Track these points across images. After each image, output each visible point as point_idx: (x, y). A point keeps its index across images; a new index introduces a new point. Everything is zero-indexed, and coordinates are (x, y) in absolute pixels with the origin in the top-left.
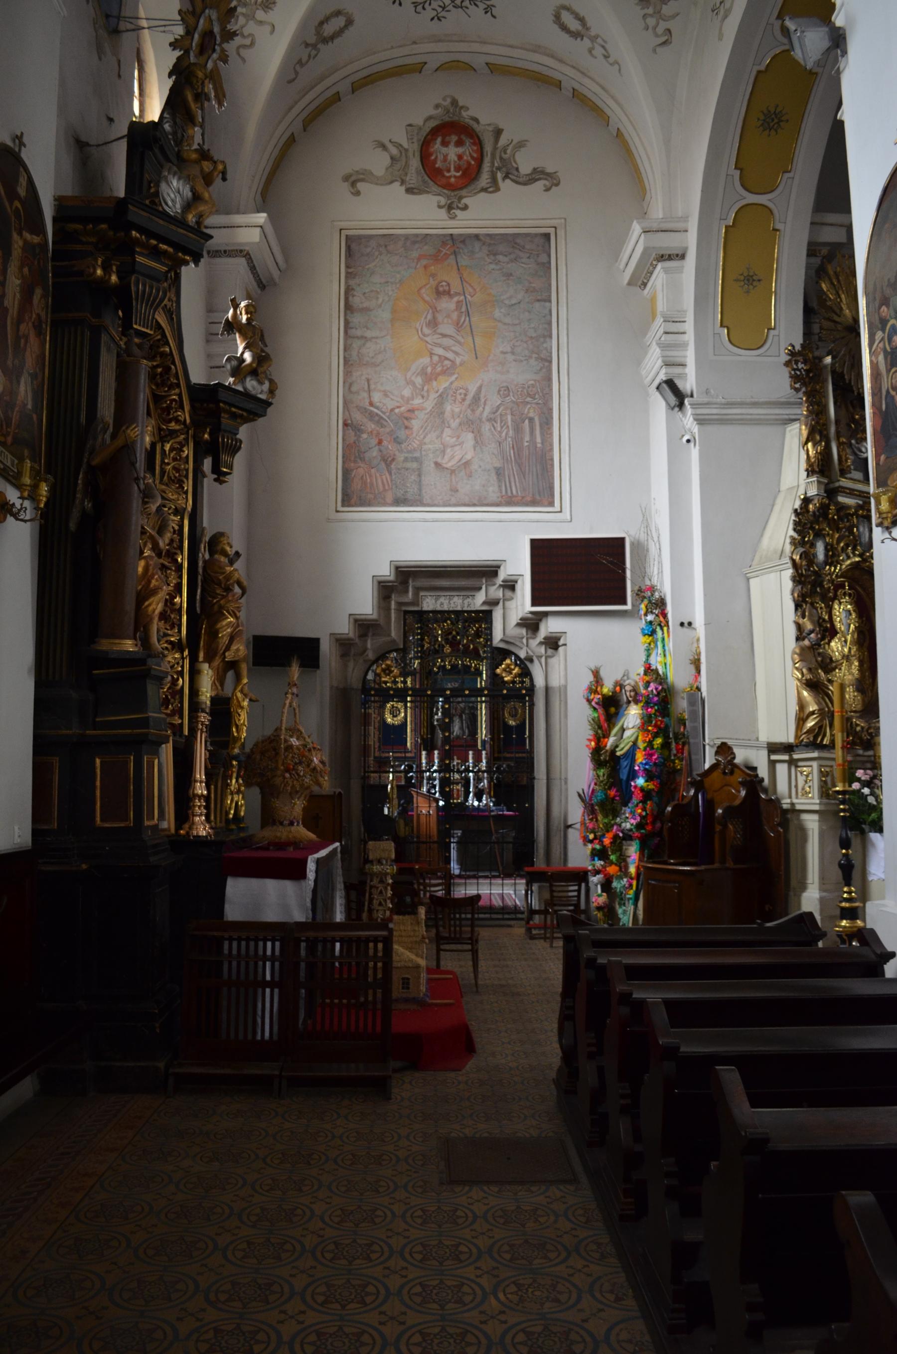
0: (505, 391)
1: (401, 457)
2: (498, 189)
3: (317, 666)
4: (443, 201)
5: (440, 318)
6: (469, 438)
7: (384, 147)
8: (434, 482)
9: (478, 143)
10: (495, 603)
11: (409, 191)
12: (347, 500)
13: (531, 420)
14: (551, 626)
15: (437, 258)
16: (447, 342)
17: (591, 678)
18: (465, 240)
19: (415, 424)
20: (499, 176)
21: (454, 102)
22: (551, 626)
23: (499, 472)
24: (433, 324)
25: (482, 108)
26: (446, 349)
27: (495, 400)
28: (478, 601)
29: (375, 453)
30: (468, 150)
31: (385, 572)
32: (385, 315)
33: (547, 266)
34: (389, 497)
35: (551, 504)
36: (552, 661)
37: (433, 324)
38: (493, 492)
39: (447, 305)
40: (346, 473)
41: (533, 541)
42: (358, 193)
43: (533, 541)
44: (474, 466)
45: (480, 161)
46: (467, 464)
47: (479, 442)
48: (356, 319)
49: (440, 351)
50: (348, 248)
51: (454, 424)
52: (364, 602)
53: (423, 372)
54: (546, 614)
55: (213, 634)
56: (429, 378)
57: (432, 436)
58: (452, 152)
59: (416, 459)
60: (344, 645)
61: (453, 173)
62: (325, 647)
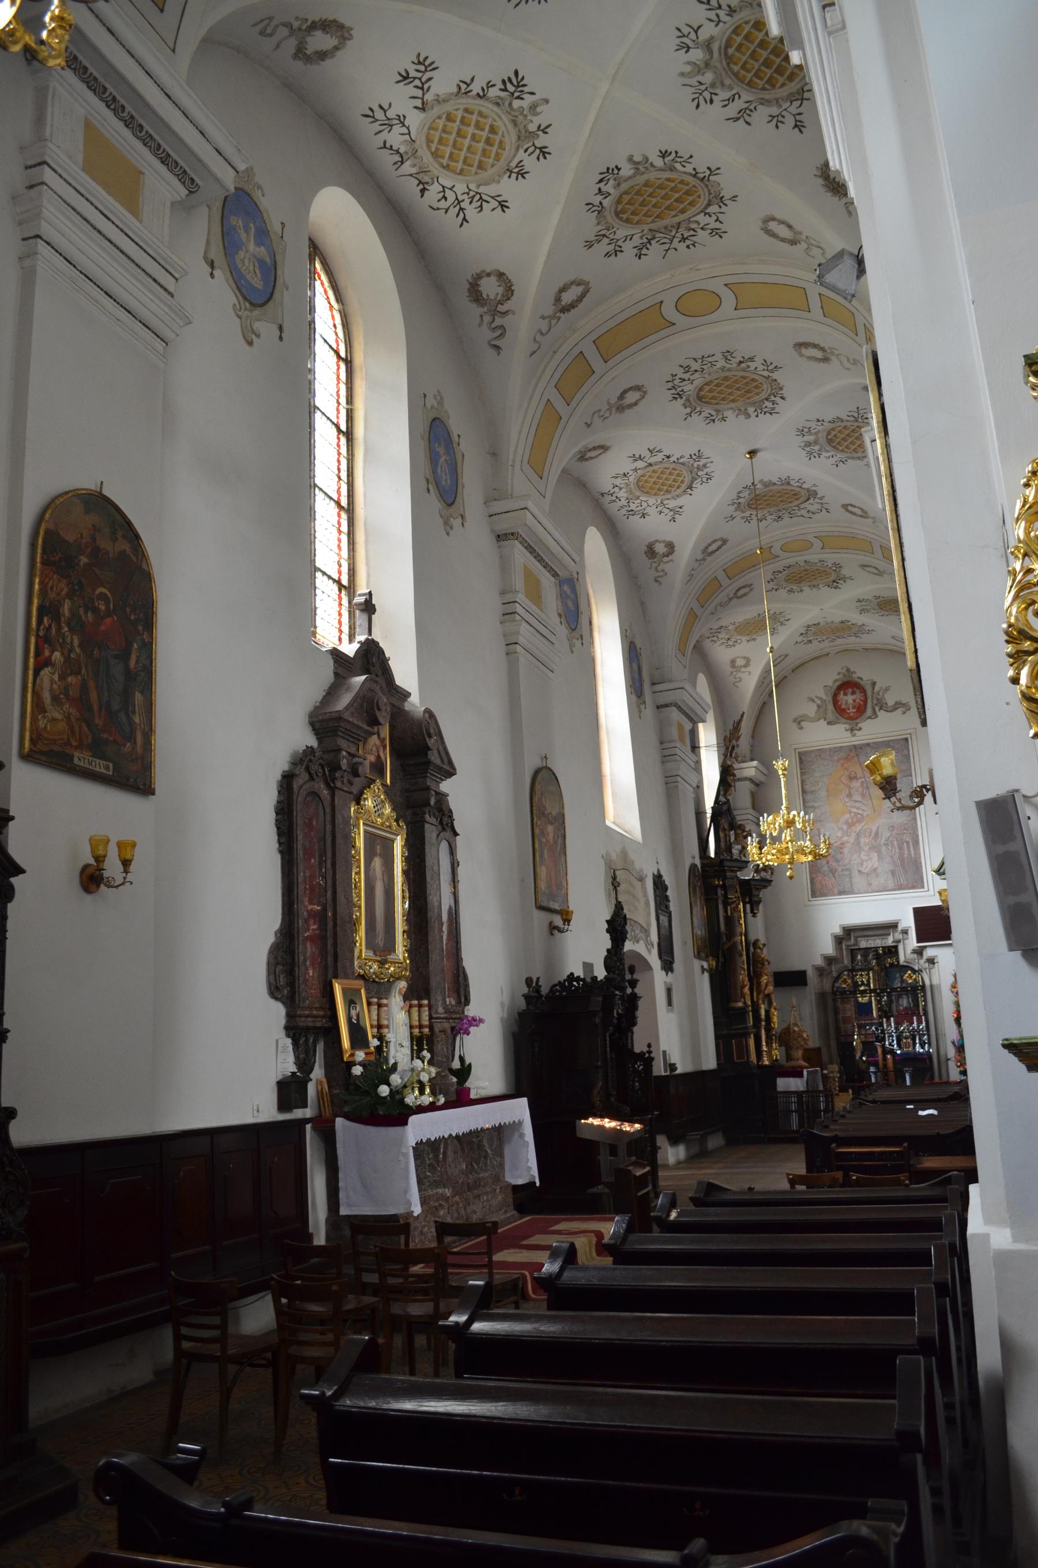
0: (892, 828)
1: (839, 869)
2: (877, 716)
3: (806, 984)
4: (848, 727)
5: (853, 792)
6: (875, 856)
7: (813, 700)
8: (858, 881)
9: (864, 691)
10: (899, 941)
11: (829, 723)
12: (814, 894)
13: (907, 842)
14: (929, 953)
15: (847, 759)
16: (858, 805)
17: (953, 979)
18: (862, 747)
19: (846, 851)
20: (877, 708)
21: (848, 670)
22: (929, 953)
23: (893, 873)
24: (850, 795)
25: (863, 673)
26: (858, 808)
27: (886, 834)
28: (890, 941)
29: (826, 868)
30: (858, 696)
31: (838, 931)
32: (824, 793)
33: (908, 756)
34: (836, 891)
35: (923, 887)
36: (933, 971)
37: (850, 795)
38: (891, 884)
39: (856, 784)
40: (812, 880)
41: (915, 909)
42: (802, 728)
43: (915, 909)
44: (879, 871)
45: (865, 701)
46: (875, 870)
47: (880, 857)
48: (808, 797)
49: (855, 810)
50: (800, 759)
51: (866, 849)
52: (828, 948)
53: (847, 823)
54: (925, 947)
55: (759, 984)
56: (850, 825)
57: (855, 856)
58: (850, 698)
59: (848, 870)
60: (820, 971)
61: (852, 710)
62: (810, 973)
